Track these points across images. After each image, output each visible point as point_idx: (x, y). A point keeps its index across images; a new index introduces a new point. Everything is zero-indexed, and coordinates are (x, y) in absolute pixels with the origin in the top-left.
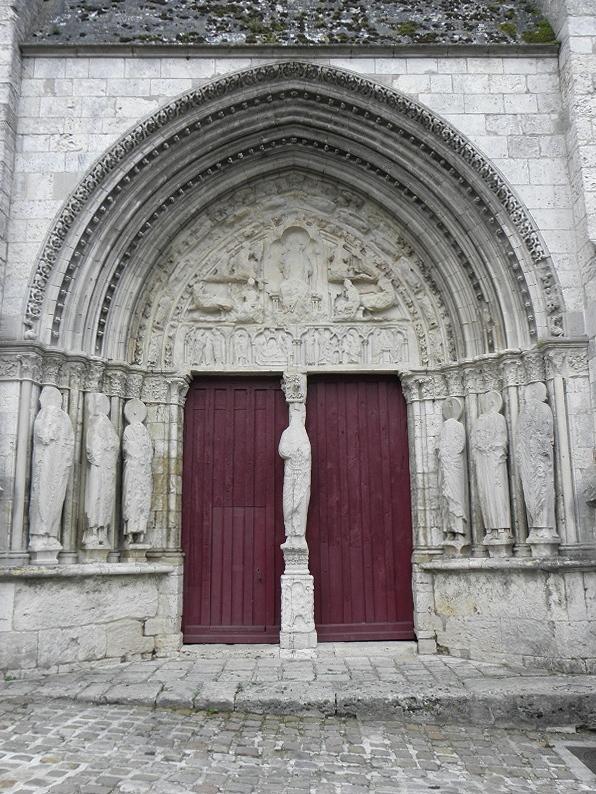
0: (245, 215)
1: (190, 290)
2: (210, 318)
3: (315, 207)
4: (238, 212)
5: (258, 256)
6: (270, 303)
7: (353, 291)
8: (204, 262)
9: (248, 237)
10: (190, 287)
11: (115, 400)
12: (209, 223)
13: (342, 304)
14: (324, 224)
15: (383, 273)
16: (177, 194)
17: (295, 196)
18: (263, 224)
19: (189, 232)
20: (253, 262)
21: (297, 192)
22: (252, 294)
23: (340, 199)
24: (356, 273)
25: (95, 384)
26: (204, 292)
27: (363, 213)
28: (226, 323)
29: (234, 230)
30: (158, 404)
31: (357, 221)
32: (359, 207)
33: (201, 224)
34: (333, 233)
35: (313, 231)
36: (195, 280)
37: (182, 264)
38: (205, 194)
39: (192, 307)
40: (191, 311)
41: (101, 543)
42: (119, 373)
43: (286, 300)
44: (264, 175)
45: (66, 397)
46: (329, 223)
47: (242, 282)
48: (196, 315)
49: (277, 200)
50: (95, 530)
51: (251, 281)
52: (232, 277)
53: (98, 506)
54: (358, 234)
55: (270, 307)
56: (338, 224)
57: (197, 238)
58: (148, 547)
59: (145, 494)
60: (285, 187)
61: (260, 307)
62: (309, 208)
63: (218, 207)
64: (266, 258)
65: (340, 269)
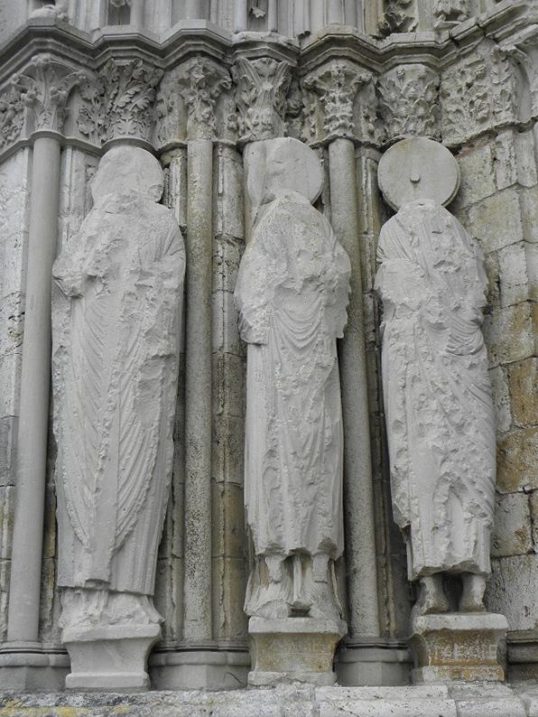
11: (340, 151)
25: (262, 113)
30: (491, 134)
41: (299, 611)
42: (334, 67)
45: (176, 170)
50: (274, 566)
53: (286, 493)
58: (496, 621)
59: (460, 428)
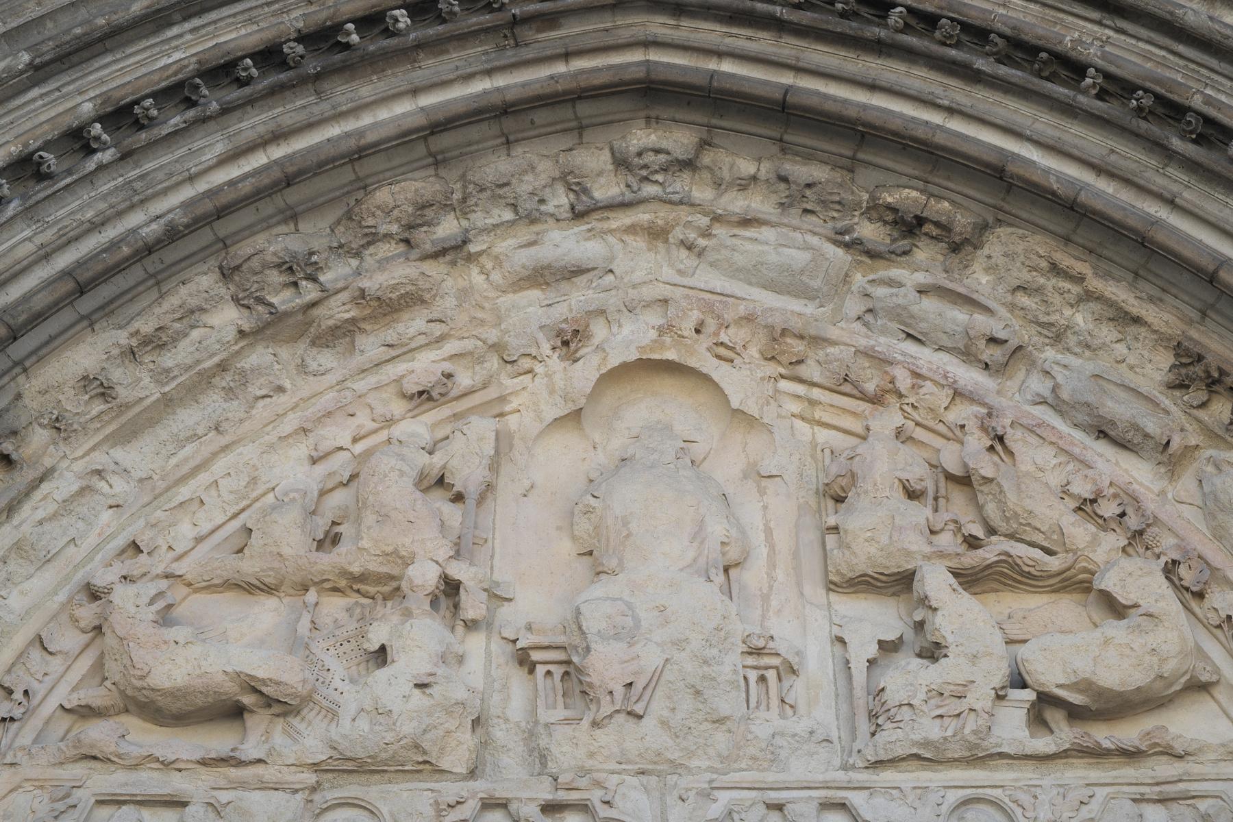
0: (412, 299)
1: (88, 613)
2: (186, 744)
3: (753, 274)
4: (375, 282)
5: (468, 475)
6: (518, 677)
7: (961, 616)
8: (185, 492)
9: (424, 397)
10: (94, 594)
12: (227, 318)
13: (907, 678)
14: (798, 347)
15: (1114, 540)
16: (77, 140)
17: (657, 234)
18: (497, 347)
19: (123, 337)
20: (439, 502)
21: (662, 215)
22: (419, 638)
23: (869, 231)
24: (972, 543)
26: (165, 618)
27: (979, 280)
28: (267, 773)
29: (358, 361)
31: (958, 316)
32: (959, 246)
33: (191, 314)
34: (845, 384)
35: (741, 382)
36: (119, 569)
37: (63, 486)
38: (209, 162)
39: (95, 696)
40: (86, 712)
43: (606, 665)
44: (505, 118)
46: (818, 341)
47: (379, 587)
48: (98, 733)
49: (566, 243)
51: (424, 575)
52: (327, 561)
54: (969, 376)
55: (516, 698)
56: (863, 342)
57: (163, 375)
60: (607, 188)
61: (461, 694)
62: (719, 282)
63: (279, 242)
64: (507, 489)
65: (883, 527)
